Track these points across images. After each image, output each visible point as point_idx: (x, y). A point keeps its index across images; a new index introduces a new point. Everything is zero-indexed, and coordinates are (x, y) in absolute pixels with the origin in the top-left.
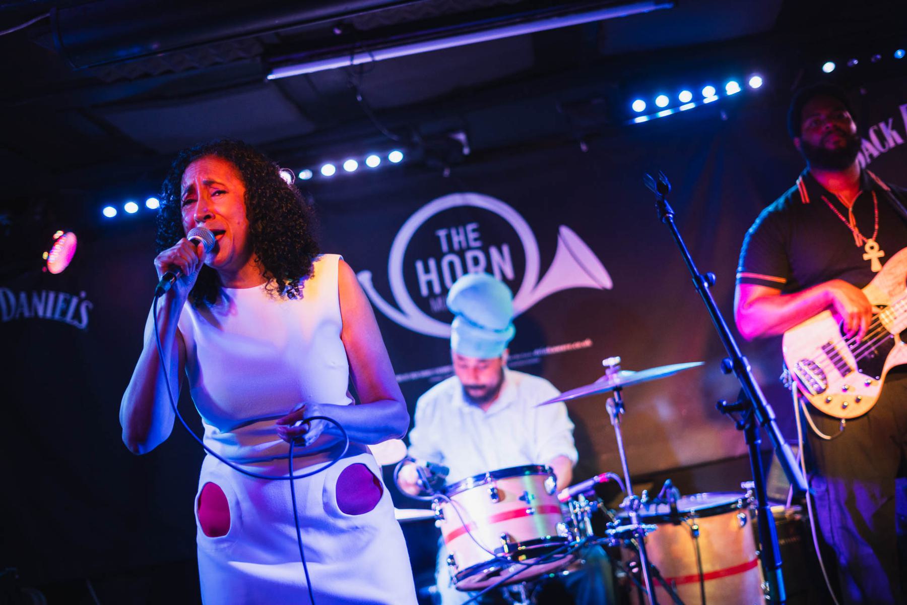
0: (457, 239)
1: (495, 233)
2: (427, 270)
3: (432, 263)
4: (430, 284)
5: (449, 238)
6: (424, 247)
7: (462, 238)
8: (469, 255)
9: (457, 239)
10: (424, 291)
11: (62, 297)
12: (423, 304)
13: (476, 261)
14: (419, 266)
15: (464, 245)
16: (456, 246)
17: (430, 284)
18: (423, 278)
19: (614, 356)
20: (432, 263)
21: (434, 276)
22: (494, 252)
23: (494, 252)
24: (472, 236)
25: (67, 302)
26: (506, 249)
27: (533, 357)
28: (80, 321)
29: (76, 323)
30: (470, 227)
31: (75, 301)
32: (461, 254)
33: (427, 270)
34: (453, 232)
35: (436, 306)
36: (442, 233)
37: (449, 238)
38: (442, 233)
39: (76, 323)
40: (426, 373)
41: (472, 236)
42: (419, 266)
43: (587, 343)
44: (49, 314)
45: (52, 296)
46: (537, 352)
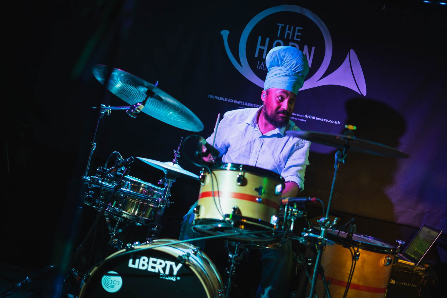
3: (268, 39)
5: (283, 29)
7: (291, 32)
10: (256, 56)
14: (260, 38)
15: (290, 38)
16: (285, 37)
18: (259, 47)
19: (353, 125)
20: (268, 39)
22: (306, 47)
23: (306, 47)
26: (313, 48)
27: (304, 118)
30: (297, 28)
34: (288, 26)
37: (283, 29)
38: (281, 25)
40: (239, 102)
42: (260, 38)
43: (339, 123)
46: (306, 116)
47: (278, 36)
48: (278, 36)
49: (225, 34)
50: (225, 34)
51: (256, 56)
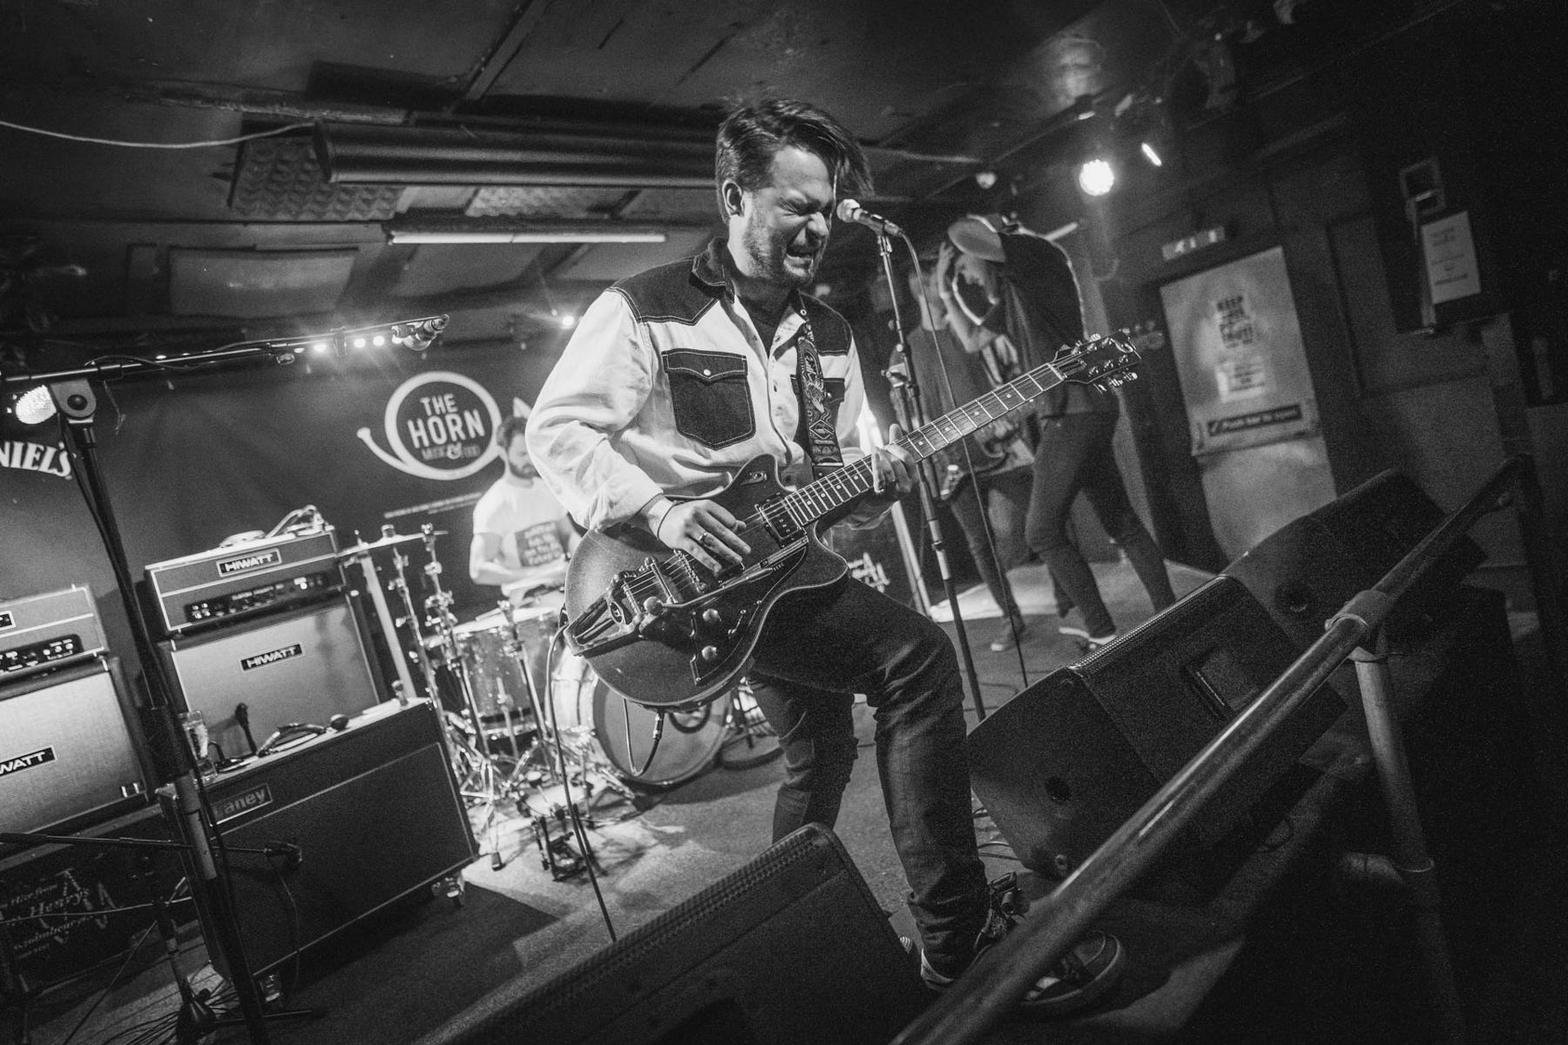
0: (438, 405)
1: (465, 401)
2: (417, 428)
3: (420, 423)
4: (420, 439)
5: (431, 404)
6: (412, 410)
8: (449, 418)
9: (438, 405)
10: (417, 444)
11: (32, 447)
12: (417, 454)
13: (454, 422)
14: (411, 424)
17: (420, 439)
18: (414, 435)
20: (420, 423)
21: (422, 433)
22: (467, 415)
23: (467, 415)
24: (449, 404)
25: (43, 454)
26: (476, 413)
28: (60, 470)
29: (54, 471)
31: (51, 451)
32: (442, 416)
33: (417, 428)
35: (428, 455)
36: (425, 401)
37: (431, 404)
39: (54, 471)
41: (449, 404)
42: (411, 424)
44: (16, 464)
45: (18, 446)
47: (429, 412)
48: (429, 412)
49: (364, 434)
50: (364, 434)
51: (417, 444)
